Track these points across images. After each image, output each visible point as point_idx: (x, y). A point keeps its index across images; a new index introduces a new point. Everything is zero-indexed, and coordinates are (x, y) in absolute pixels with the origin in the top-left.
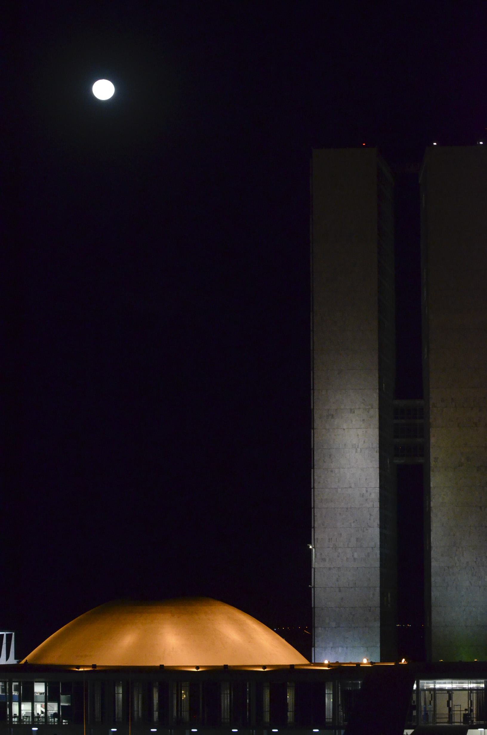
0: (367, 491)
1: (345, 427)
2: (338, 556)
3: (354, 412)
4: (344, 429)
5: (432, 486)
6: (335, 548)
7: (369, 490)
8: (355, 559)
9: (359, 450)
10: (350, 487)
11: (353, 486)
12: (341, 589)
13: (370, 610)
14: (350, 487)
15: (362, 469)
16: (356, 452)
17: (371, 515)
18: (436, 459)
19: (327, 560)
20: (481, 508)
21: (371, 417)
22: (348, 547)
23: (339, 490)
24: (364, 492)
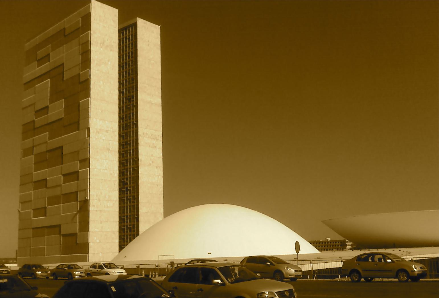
0: (113, 172)
1: (104, 139)
2: (101, 204)
3: (108, 132)
4: (103, 140)
5: (139, 173)
6: (99, 200)
7: (114, 172)
8: (108, 207)
9: (110, 151)
10: (106, 169)
11: (107, 169)
12: (102, 222)
13: (114, 233)
14: (106, 169)
15: (111, 161)
16: (109, 152)
17: (115, 184)
18: (141, 160)
19: (96, 206)
20: (158, 186)
21: (115, 136)
22: (105, 200)
23: (101, 170)
24: (112, 172)
